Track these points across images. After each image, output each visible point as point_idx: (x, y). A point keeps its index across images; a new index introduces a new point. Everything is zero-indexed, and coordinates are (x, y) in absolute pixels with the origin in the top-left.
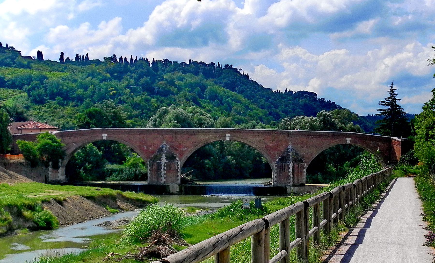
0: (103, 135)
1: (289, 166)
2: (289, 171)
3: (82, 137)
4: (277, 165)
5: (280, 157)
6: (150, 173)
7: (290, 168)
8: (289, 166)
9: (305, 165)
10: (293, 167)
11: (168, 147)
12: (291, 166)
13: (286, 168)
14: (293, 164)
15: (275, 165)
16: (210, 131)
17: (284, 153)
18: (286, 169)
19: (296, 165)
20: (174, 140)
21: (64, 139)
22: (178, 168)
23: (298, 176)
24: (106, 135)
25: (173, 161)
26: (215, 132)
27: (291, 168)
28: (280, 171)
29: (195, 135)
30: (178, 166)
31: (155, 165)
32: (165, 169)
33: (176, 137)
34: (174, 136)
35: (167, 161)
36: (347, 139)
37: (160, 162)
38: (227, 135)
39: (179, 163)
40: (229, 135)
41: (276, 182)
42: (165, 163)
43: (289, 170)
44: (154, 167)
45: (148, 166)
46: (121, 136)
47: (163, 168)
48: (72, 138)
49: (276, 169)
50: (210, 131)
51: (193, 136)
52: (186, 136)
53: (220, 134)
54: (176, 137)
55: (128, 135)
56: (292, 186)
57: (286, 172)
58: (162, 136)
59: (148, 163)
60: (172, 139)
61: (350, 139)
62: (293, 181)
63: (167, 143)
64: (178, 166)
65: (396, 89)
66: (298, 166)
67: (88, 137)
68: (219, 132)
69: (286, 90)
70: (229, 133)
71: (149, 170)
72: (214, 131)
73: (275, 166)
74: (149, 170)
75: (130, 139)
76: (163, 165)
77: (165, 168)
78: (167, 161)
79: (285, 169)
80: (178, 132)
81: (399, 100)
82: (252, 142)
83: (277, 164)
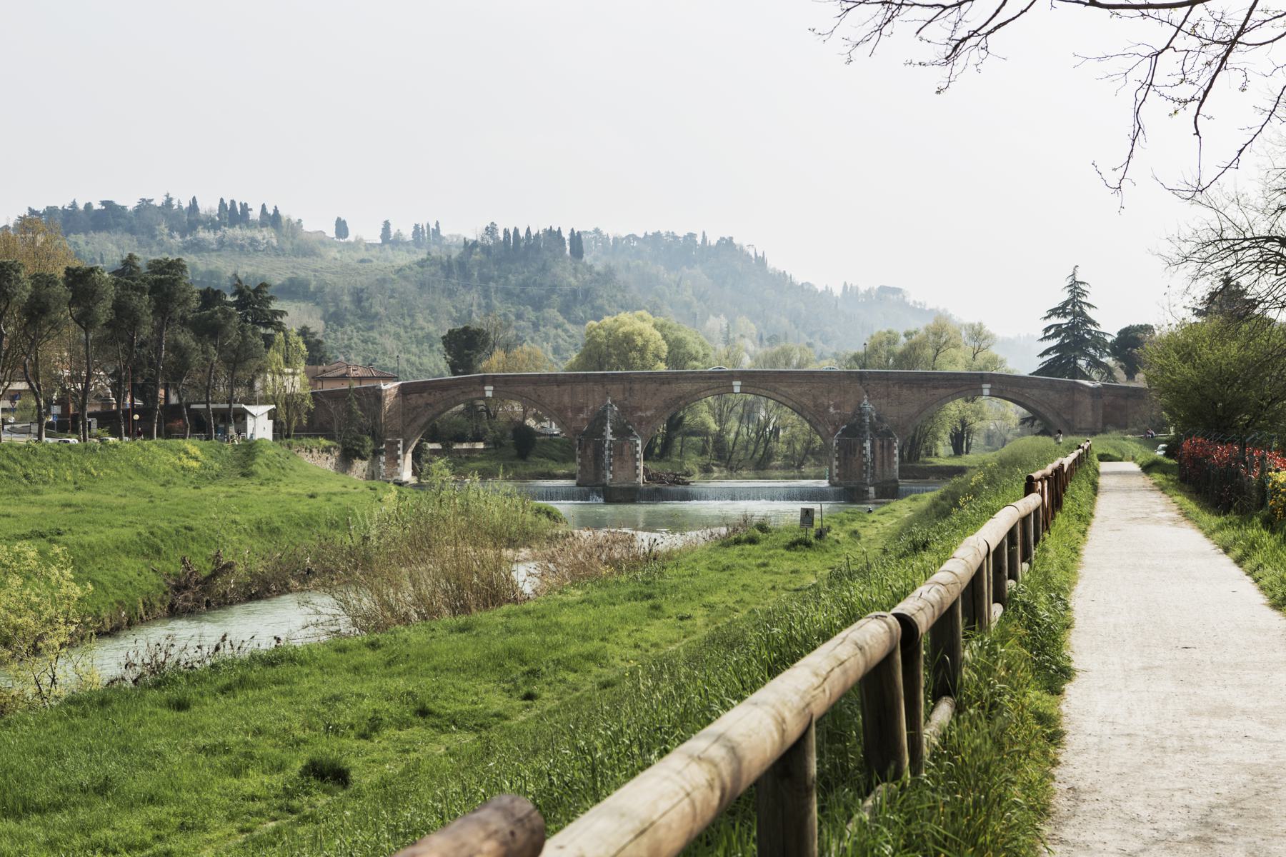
0: (486, 388)
3: (445, 394)
5: (845, 427)
7: (865, 448)
10: (873, 446)
12: (868, 445)
17: (854, 416)
19: (878, 443)
20: (627, 394)
21: (409, 397)
22: (637, 452)
24: (492, 388)
26: (710, 378)
27: (869, 449)
28: (846, 454)
29: (669, 383)
34: (628, 386)
36: (984, 386)
38: (734, 383)
39: (639, 442)
40: (739, 383)
44: (589, 452)
46: (519, 389)
47: (607, 453)
48: (425, 395)
49: (836, 452)
52: (652, 387)
59: (577, 442)
61: (989, 386)
62: (873, 475)
63: (614, 402)
65: (1081, 283)
68: (719, 378)
76: (606, 446)
79: (855, 450)
81: (1089, 305)
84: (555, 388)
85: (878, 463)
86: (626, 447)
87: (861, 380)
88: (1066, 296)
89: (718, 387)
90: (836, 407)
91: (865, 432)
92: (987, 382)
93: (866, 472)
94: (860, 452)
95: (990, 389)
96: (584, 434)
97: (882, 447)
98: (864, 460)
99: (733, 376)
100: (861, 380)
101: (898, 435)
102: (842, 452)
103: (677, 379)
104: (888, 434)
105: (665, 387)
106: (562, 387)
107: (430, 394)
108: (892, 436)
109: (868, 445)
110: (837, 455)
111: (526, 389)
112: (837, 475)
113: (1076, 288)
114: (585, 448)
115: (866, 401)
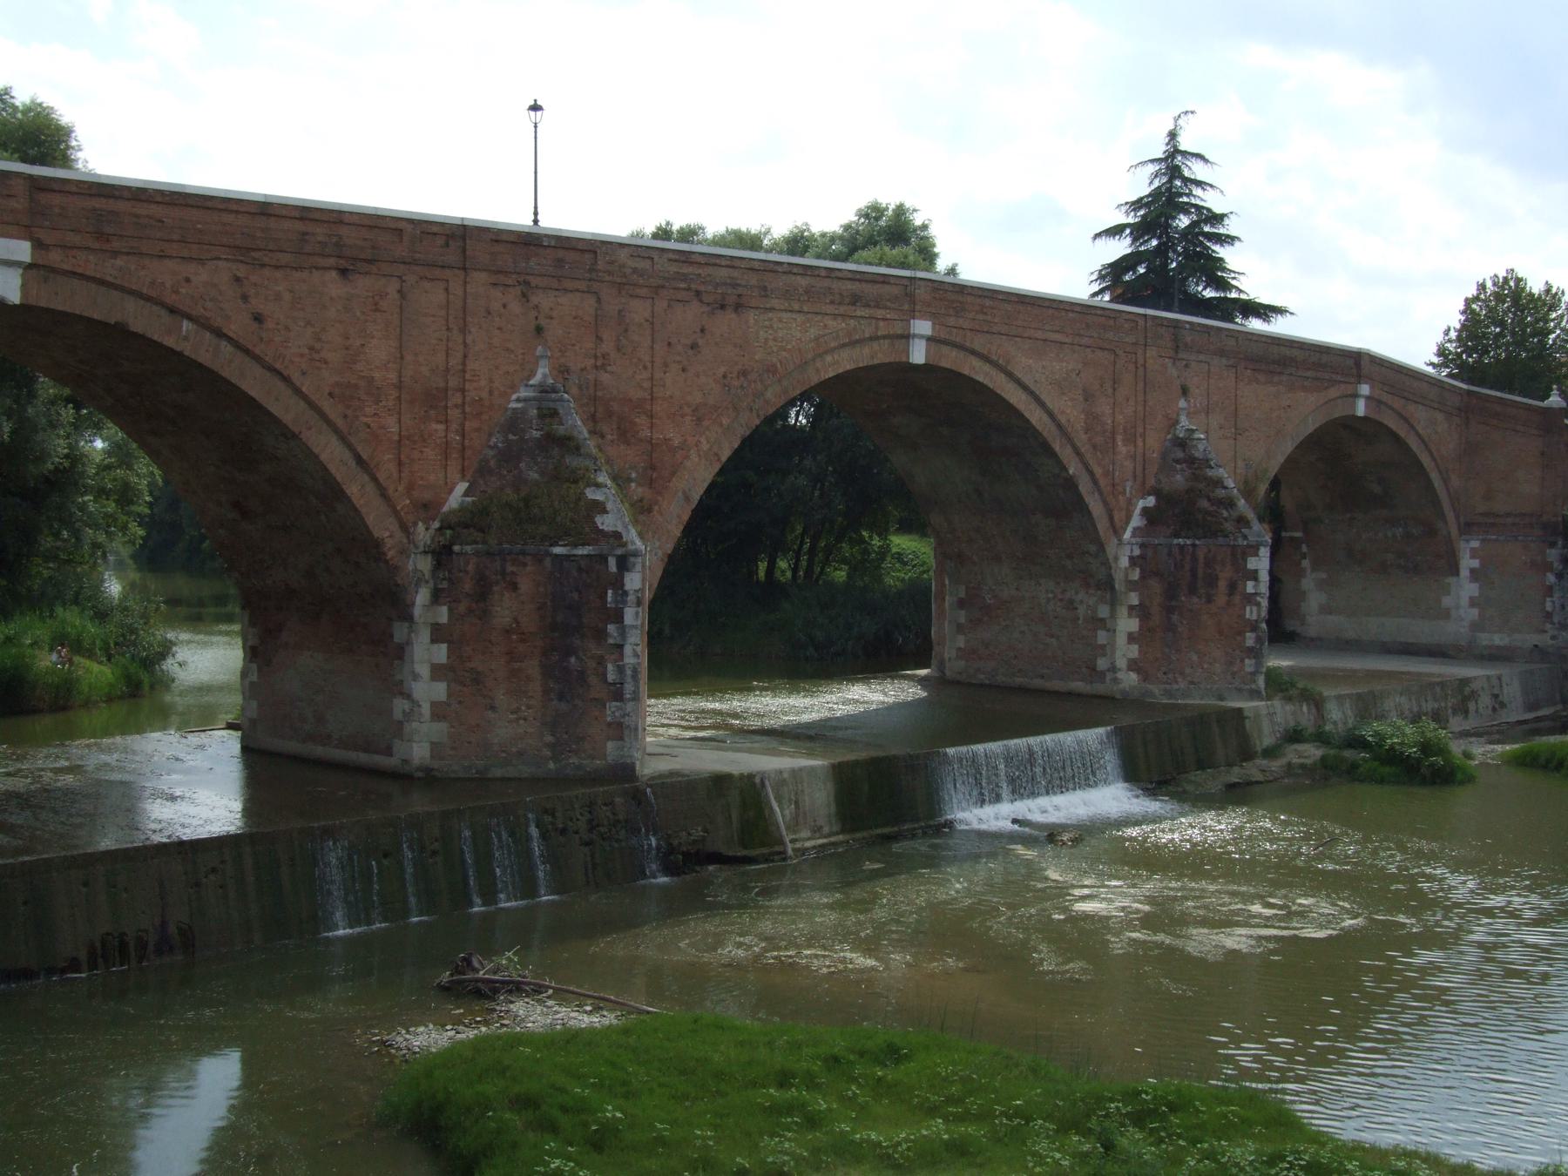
1: (1252, 563)
2: (1250, 599)
4: (1142, 557)
5: (1151, 501)
6: (437, 672)
7: (1254, 576)
8: (1252, 563)
13: (1225, 575)
16: (827, 283)
20: (607, 346)
26: (855, 300)
28: (1171, 593)
29: (738, 307)
31: (525, 585)
37: (603, 559)
41: (1133, 676)
45: (422, 597)
49: (1132, 586)
51: (730, 315)
53: (880, 313)
55: (241, 271)
57: (1221, 600)
59: (425, 564)
60: (599, 339)
63: (563, 371)
71: (435, 640)
73: (1124, 562)
74: (435, 640)
75: (258, 318)
79: (1212, 581)
80: (635, 270)
82: (1032, 386)
83: (1142, 546)
84: (333, 286)
87: (1177, 349)
88: (1141, 185)
92: (1369, 379)
94: (1233, 587)
96: (470, 521)
98: (1251, 613)
99: (911, 297)
102: (1156, 586)
105: (725, 322)
106: (363, 285)
110: (1134, 599)
111: (201, 275)
112: (1133, 665)
113: (1172, 163)
114: (483, 591)
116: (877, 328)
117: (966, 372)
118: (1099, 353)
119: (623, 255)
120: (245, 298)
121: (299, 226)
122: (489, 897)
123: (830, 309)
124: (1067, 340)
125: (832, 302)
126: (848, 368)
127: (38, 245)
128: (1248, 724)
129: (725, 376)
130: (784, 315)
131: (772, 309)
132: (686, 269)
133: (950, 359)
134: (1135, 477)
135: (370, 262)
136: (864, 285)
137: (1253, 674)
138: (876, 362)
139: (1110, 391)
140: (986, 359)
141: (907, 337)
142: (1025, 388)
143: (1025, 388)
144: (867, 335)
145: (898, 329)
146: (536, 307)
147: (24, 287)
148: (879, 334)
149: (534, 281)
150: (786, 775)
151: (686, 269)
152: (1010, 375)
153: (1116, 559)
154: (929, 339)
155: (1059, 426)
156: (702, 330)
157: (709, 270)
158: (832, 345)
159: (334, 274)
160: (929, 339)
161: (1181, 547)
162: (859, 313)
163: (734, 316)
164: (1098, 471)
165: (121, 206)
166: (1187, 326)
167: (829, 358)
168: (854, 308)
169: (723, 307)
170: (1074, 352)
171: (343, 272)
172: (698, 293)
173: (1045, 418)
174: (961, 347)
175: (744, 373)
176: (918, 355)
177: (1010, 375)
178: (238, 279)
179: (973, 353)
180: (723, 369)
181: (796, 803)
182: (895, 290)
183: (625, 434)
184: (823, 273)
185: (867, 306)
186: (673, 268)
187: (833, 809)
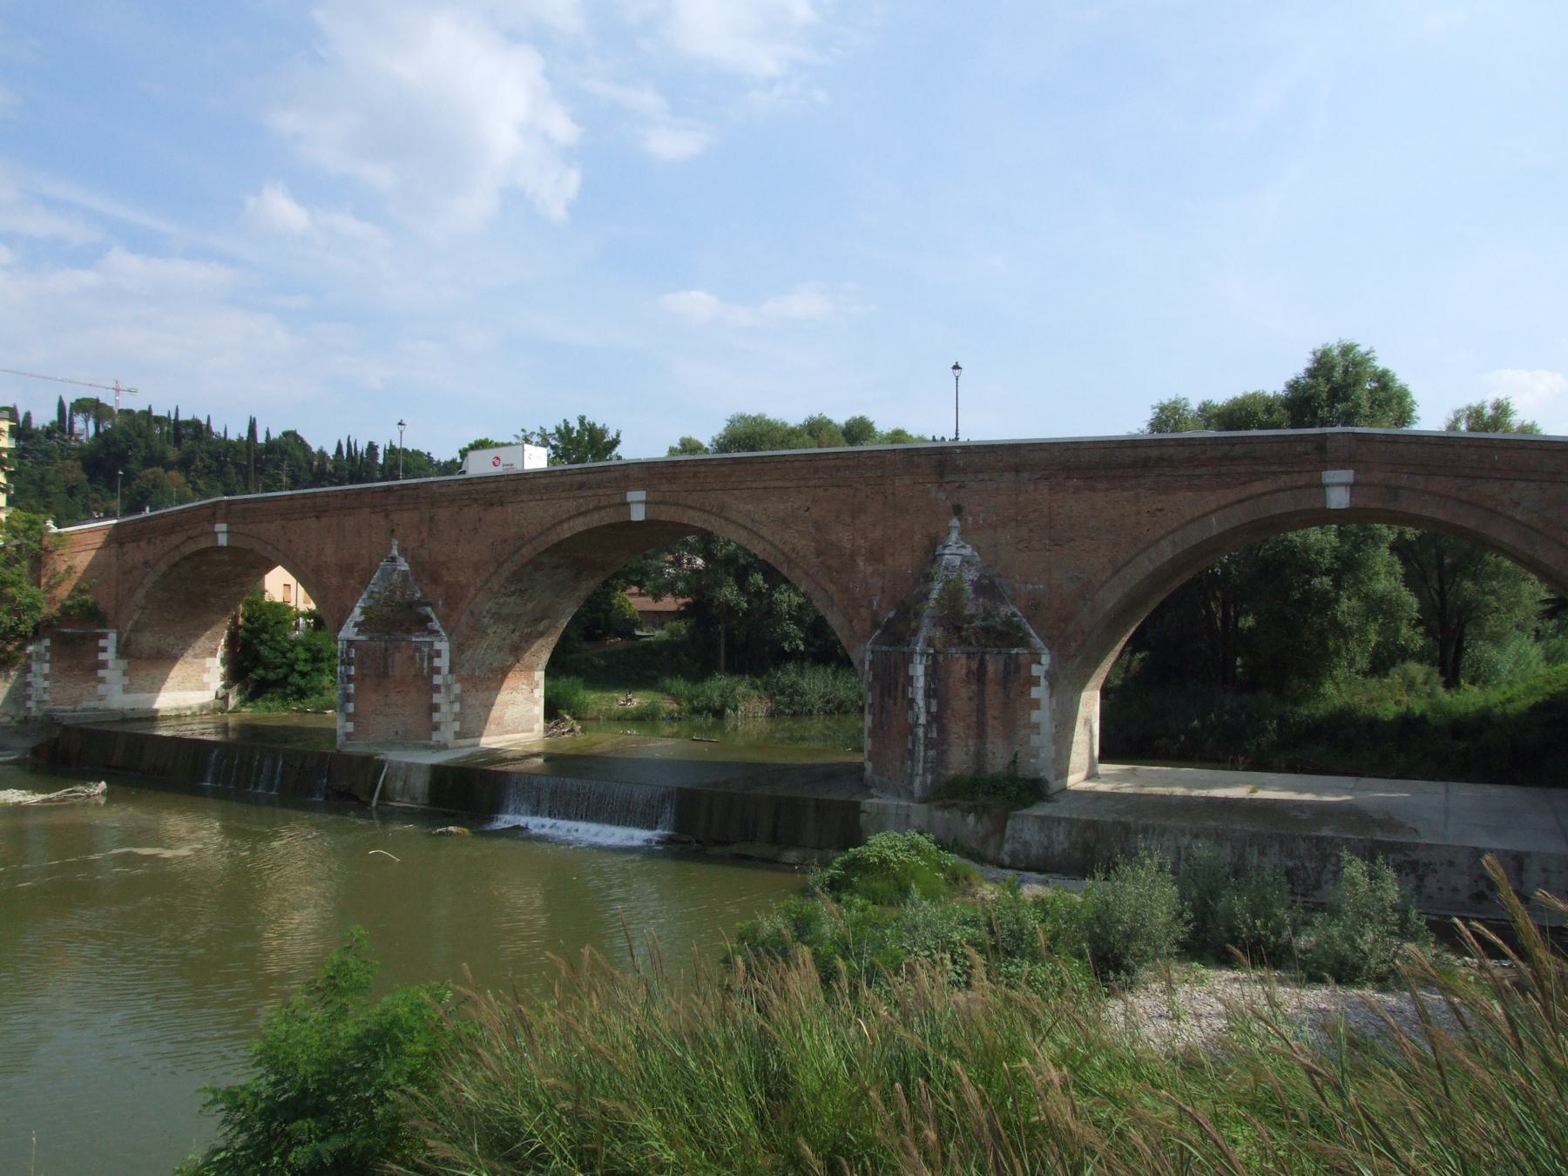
5: (891, 614)
9: (1046, 659)
10: (934, 673)
11: (404, 566)
12: (918, 670)
14: (935, 662)
15: (869, 657)
16: (562, 479)
18: (900, 688)
19: (960, 664)
21: (125, 550)
23: (981, 732)
25: (405, 636)
26: (581, 486)
27: (920, 683)
29: (502, 504)
30: (437, 662)
32: (353, 673)
33: (432, 519)
35: (362, 638)
36: (1330, 476)
42: (351, 643)
43: (910, 696)
48: (143, 544)
50: (562, 479)
53: (601, 492)
54: (432, 519)
56: (924, 800)
57: (899, 700)
58: (387, 516)
60: (421, 532)
61: (1347, 475)
64: (437, 662)
66: (974, 665)
67: (176, 539)
69: (1418, 418)
70: (640, 484)
72: (579, 478)
75: (290, 541)
77: (353, 671)
78: (362, 638)
85: (956, 729)
86: (398, 658)
87: (941, 475)
89: (598, 508)
90: (876, 556)
91: (915, 632)
92: (1342, 464)
93: (911, 754)
95: (1353, 487)
97: (979, 676)
100: (941, 475)
101: (1050, 641)
103: (516, 491)
104: (1009, 635)
107: (149, 542)
108: (1024, 641)
109: (918, 670)
115: (954, 536)
116: (599, 502)
117: (686, 522)
118: (835, 490)
119: (435, 486)
120: (285, 534)
121: (302, 501)
122: (256, 787)
123: (564, 494)
124: (790, 485)
125: (563, 491)
126: (581, 529)
127: (230, 524)
128: (863, 817)
129: (492, 544)
130: (532, 504)
131: (522, 501)
132: (471, 488)
133: (667, 514)
134: (883, 591)
135: (325, 511)
136: (591, 476)
137: (911, 775)
138: (603, 523)
139: (849, 520)
140: (702, 510)
141: (627, 504)
142: (745, 527)
143: (745, 527)
144: (591, 507)
145: (617, 499)
146: (392, 521)
147: (228, 539)
148: (602, 504)
149: (390, 508)
150: (402, 765)
151: (471, 488)
152: (727, 519)
153: (862, 663)
154: (646, 503)
155: (784, 554)
156: (480, 520)
157: (484, 485)
158: (564, 517)
159: (314, 519)
160: (646, 503)
161: (886, 653)
162: (584, 494)
163: (499, 509)
164: (832, 588)
165: (251, 506)
166: (958, 451)
167: (566, 525)
168: (580, 492)
169: (492, 505)
170: (801, 492)
171: (317, 517)
172: (476, 500)
173: (769, 548)
174: (677, 504)
175: (506, 541)
176: (638, 514)
177: (727, 519)
178: (284, 527)
179: (689, 507)
180: (491, 541)
181: (405, 782)
182: (617, 474)
183: (435, 579)
184: (557, 474)
185: (590, 488)
186: (464, 488)
187: (426, 791)
